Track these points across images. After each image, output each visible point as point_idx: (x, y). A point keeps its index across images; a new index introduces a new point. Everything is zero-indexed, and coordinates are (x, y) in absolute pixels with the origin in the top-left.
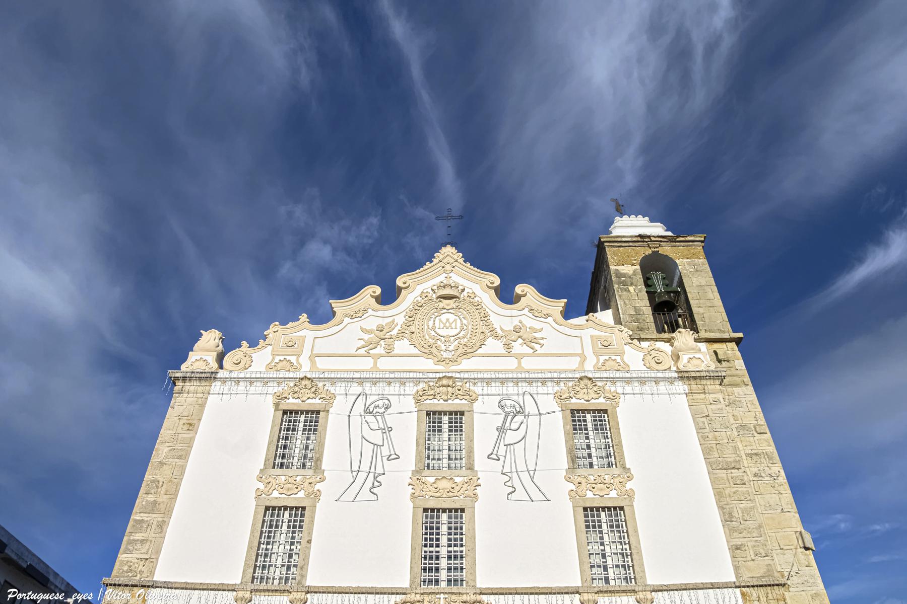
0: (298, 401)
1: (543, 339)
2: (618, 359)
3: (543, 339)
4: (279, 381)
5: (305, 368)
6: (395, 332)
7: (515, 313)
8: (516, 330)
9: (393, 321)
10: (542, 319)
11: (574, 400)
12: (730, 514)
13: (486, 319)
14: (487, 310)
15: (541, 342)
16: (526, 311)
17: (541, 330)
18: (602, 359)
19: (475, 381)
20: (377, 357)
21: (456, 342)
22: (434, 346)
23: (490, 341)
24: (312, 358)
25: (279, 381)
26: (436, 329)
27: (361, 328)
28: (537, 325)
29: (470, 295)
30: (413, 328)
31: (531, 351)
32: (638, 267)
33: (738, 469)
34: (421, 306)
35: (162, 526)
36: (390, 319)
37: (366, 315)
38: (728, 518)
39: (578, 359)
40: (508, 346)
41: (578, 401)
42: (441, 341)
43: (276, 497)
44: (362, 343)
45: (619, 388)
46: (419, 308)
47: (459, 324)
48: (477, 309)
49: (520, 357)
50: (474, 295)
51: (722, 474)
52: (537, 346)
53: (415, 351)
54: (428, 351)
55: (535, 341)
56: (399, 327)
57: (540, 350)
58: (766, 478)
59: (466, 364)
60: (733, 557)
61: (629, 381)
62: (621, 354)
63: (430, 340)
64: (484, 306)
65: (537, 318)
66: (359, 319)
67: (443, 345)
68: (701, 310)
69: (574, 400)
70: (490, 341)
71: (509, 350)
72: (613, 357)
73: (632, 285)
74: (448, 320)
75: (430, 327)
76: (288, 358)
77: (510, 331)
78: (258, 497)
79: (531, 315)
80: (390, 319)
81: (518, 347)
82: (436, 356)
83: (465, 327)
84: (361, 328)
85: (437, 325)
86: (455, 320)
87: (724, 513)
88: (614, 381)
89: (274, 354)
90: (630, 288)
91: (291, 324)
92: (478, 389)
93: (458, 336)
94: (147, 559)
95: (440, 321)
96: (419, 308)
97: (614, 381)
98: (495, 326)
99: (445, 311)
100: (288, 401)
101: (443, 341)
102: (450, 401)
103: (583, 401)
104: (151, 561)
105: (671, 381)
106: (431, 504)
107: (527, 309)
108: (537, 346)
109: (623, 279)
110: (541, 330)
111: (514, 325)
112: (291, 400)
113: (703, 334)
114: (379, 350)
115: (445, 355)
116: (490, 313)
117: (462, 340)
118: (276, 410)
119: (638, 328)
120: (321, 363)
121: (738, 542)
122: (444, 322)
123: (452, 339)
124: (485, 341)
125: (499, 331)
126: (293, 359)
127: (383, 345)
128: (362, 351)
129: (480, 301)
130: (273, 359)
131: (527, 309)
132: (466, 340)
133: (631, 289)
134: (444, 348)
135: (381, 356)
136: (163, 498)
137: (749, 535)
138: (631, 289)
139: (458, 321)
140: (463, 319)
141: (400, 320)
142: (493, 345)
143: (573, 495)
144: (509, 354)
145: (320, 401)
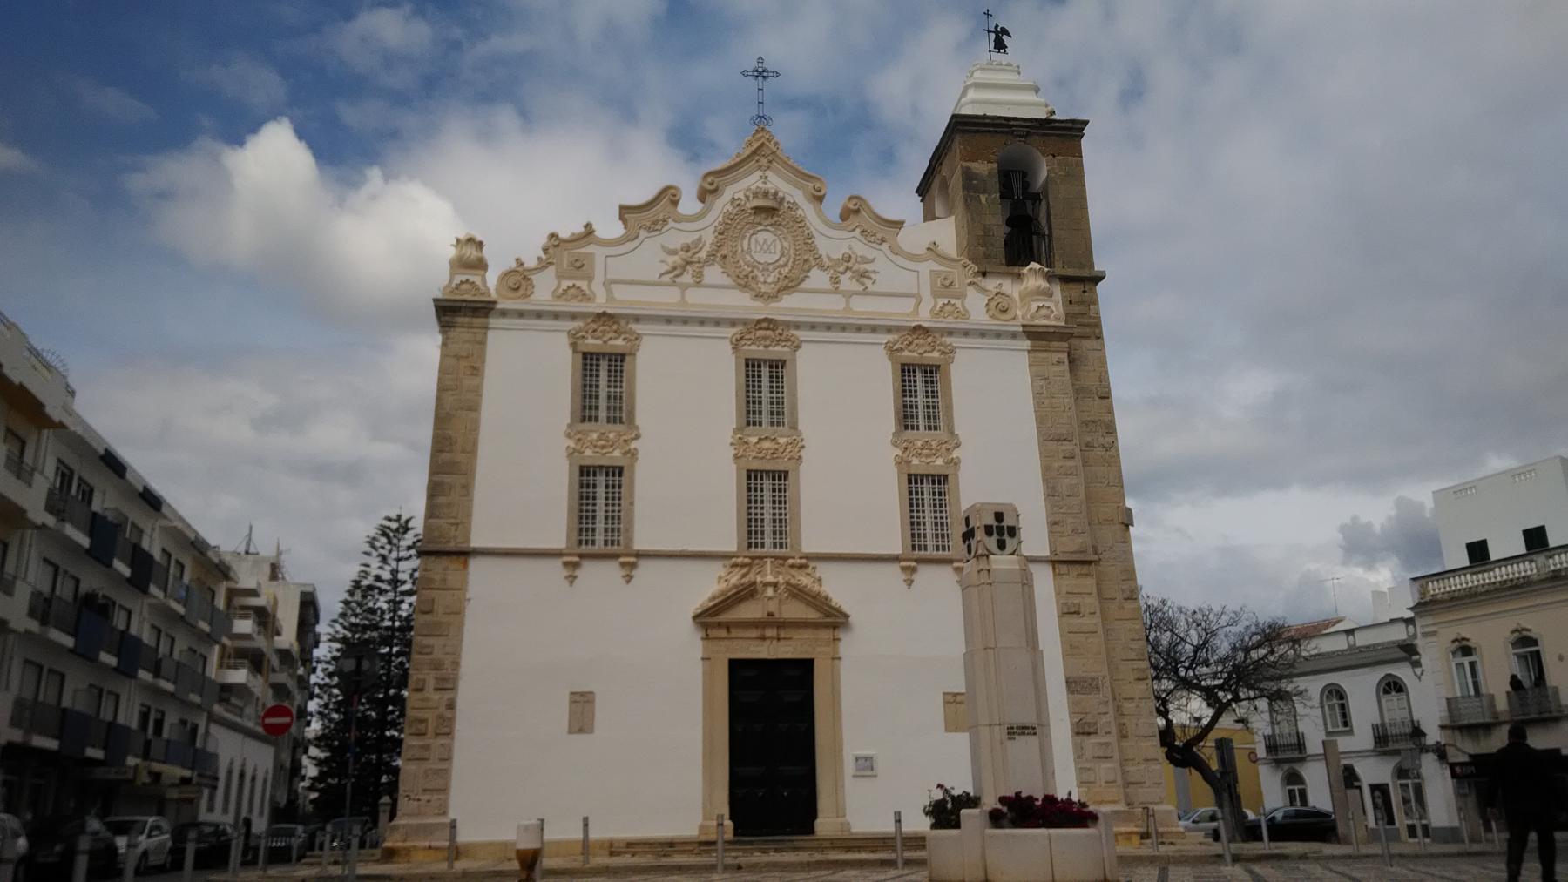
0: (599, 342)
1: (875, 272)
2: (958, 303)
3: (875, 272)
4: (573, 316)
5: (600, 303)
6: (703, 255)
7: (844, 234)
8: (847, 259)
9: (700, 239)
10: (874, 245)
11: (906, 353)
12: (1053, 488)
13: (810, 241)
14: (812, 229)
15: (873, 276)
17: (873, 261)
19: (798, 326)
20: (685, 287)
21: (776, 273)
22: (751, 275)
24: (608, 283)
25: (573, 316)
26: (753, 254)
27: (663, 247)
28: (870, 254)
29: (791, 206)
30: (724, 252)
31: (862, 288)
32: (995, 165)
33: (1070, 441)
34: (732, 219)
37: (666, 228)
39: (913, 301)
40: (835, 281)
41: (910, 354)
42: (758, 269)
43: (590, 456)
44: (666, 268)
45: (954, 341)
46: (729, 222)
47: (779, 248)
48: (800, 227)
50: (794, 206)
51: (1052, 445)
53: (729, 281)
54: (744, 282)
55: (864, 275)
56: (707, 248)
57: (871, 288)
58: (1098, 449)
60: (1051, 533)
61: (966, 333)
62: (962, 296)
63: (746, 267)
64: (808, 224)
65: (870, 244)
66: (658, 232)
67: (760, 275)
69: (906, 353)
71: (836, 286)
72: (953, 301)
74: (765, 241)
75: (745, 248)
76: (578, 283)
77: (839, 259)
78: (570, 455)
79: (863, 239)
80: (696, 235)
81: (847, 282)
82: (752, 289)
83: (786, 252)
84: (663, 247)
86: (774, 241)
87: (1048, 487)
88: (951, 333)
92: (802, 335)
93: (777, 264)
94: (458, 524)
95: (757, 241)
96: (729, 222)
97: (951, 333)
100: (586, 342)
101: (761, 269)
102: (771, 348)
103: (915, 354)
105: (1014, 336)
106: (755, 465)
107: (858, 230)
108: (868, 283)
109: (975, 182)
110: (873, 261)
111: (843, 252)
112: (590, 341)
113: (1059, 271)
114: (687, 278)
115: (764, 289)
116: (814, 233)
117: (782, 270)
118: (575, 351)
119: (985, 254)
120: (620, 293)
122: (761, 243)
123: (771, 267)
124: (809, 271)
126: (583, 285)
127: (691, 272)
128: (666, 278)
129: (803, 215)
130: (558, 286)
131: (858, 230)
132: (787, 269)
133: (983, 198)
134: (762, 279)
136: (460, 457)
137: (1069, 511)
138: (983, 198)
139: (778, 242)
140: (783, 241)
141: (709, 238)
142: (818, 278)
143: (901, 463)
144: (836, 291)
145: (624, 343)
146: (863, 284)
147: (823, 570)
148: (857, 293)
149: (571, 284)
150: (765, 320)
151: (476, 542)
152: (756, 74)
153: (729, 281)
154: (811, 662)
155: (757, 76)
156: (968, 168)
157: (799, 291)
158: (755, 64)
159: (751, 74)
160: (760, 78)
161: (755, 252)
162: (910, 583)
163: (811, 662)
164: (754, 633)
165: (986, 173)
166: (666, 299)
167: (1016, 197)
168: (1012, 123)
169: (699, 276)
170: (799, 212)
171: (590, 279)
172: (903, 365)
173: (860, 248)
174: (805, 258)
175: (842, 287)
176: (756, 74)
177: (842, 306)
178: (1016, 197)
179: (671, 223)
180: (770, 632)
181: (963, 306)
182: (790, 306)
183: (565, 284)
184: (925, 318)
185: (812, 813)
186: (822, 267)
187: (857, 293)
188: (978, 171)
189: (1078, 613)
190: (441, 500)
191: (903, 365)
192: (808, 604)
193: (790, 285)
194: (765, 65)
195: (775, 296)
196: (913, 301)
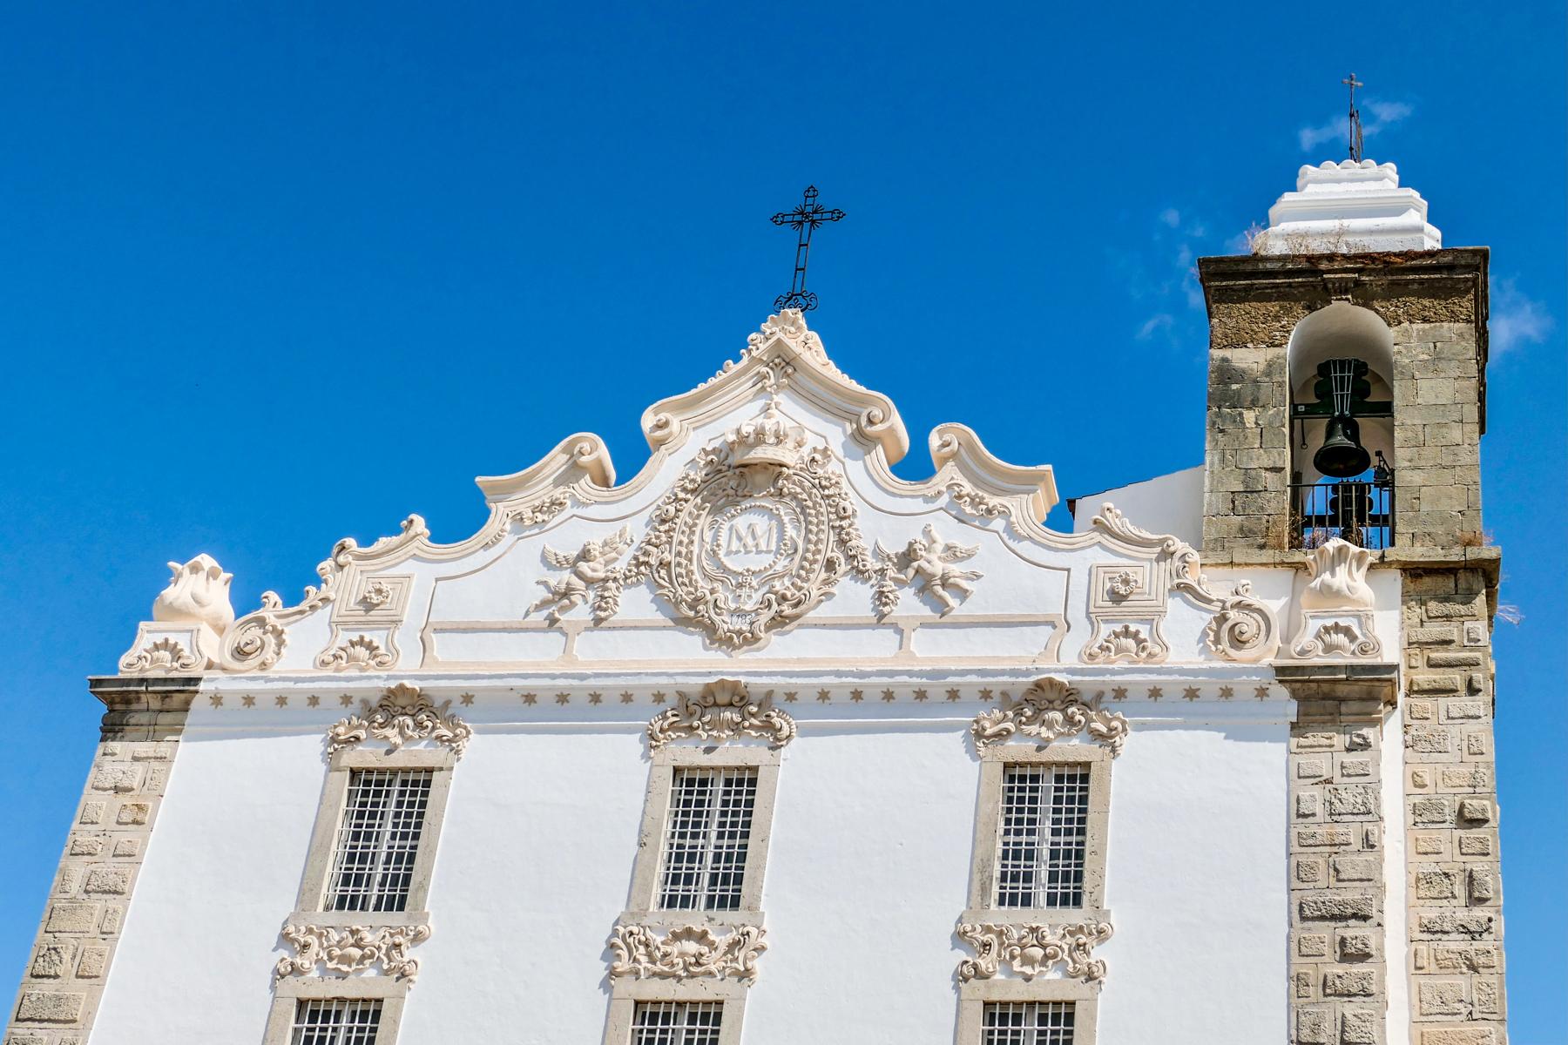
6: (621, 566)
7: (917, 505)
8: (907, 558)
18: (1105, 630)
58: (1454, 936)
68: (1417, 478)
73: (1254, 404)
81: (907, 603)
90: (1245, 412)
91: (383, 542)
98: (862, 543)
109: (1234, 387)
113: (1405, 550)
114: (581, 612)
119: (1241, 529)
133: (1249, 416)
138: (1249, 416)
141: (638, 530)
149: (355, 637)
152: (798, 218)
155: (800, 223)
157: (800, 626)
158: (798, 201)
159: (790, 218)
160: (807, 225)
161: (728, 553)
165: (1262, 367)
167: (1337, 413)
172: (1007, 766)
173: (946, 530)
175: (896, 612)
176: (798, 218)
178: (1337, 413)
186: (859, 573)
188: (1243, 365)
191: (1007, 766)
194: (819, 201)
195: (751, 640)
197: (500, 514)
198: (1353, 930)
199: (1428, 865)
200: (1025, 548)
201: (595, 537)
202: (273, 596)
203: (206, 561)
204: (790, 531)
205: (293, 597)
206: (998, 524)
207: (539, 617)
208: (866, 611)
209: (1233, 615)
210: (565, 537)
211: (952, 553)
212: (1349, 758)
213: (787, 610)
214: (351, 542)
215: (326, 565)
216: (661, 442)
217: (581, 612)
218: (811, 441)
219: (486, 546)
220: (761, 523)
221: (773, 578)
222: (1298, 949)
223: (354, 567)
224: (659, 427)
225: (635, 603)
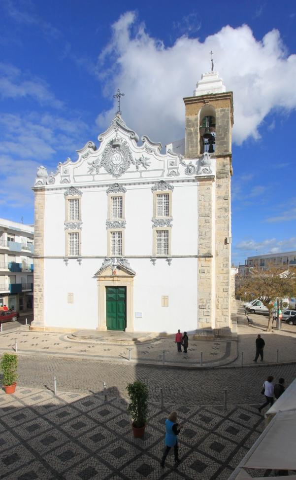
1: (150, 163)
3: (150, 163)
5: (72, 184)
6: (99, 164)
7: (141, 151)
9: (98, 159)
15: (149, 164)
16: (144, 150)
20: (94, 175)
23: (131, 165)
35: (42, 240)
36: (97, 158)
38: (200, 235)
39: (162, 171)
44: (88, 169)
49: (141, 172)
51: (203, 219)
52: (147, 167)
54: (110, 171)
56: (100, 161)
59: (123, 176)
62: (177, 168)
70: (131, 165)
80: (97, 158)
81: (141, 168)
84: (88, 163)
85: (113, 159)
88: (173, 182)
89: (61, 177)
91: (65, 162)
92: (127, 187)
99: (115, 152)
104: (42, 250)
105: (194, 181)
108: (147, 167)
114: (95, 172)
121: (201, 242)
125: (135, 160)
126: (67, 178)
131: (145, 149)
135: (95, 175)
141: (101, 157)
142: (132, 167)
144: (137, 171)
146: (146, 168)
147: (130, 260)
148: (144, 171)
150: (116, 184)
151: (45, 255)
153: (106, 172)
154: (125, 287)
156: (188, 118)
162: (154, 264)
163: (125, 287)
164: (112, 279)
166: (88, 180)
168: (204, 97)
169: (98, 171)
170: (127, 144)
171: (69, 176)
173: (146, 155)
174: (128, 160)
177: (139, 176)
179: (90, 155)
180: (115, 279)
181: (177, 171)
182: (124, 178)
183: (63, 178)
184: (165, 178)
185: (125, 326)
186: (133, 163)
187: (144, 171)
189: (204, 273)
190: (37, 244)
192: (125, 271)
193: (123, 170)
195: (119, 175)
196: (162, 171)
197: (80, 155)
198: (207, 218)
199: (219, 207)
200: (157, 157)
201: (94, 159)
202: (52, 173)
203: (42, 167)
204: (123, 157)
205: (55, 172)
206: (153, 153)
207: (89, 173)
208: (135, 170)
209: (190, 167)
210: (91, 159)
211: (147, 159)
212: (207, 191)
213: (124, 170)
214: (61, 163)
215: (58, 167)
216: (101, 142)
217: (95, 172)
218: (124, 140)
219: (80, 162)
220: (118, 155)
221: (121, 165)
222: (199, 221)
223: (62, 166)
224: (100, 139)
225: (102, 170)
